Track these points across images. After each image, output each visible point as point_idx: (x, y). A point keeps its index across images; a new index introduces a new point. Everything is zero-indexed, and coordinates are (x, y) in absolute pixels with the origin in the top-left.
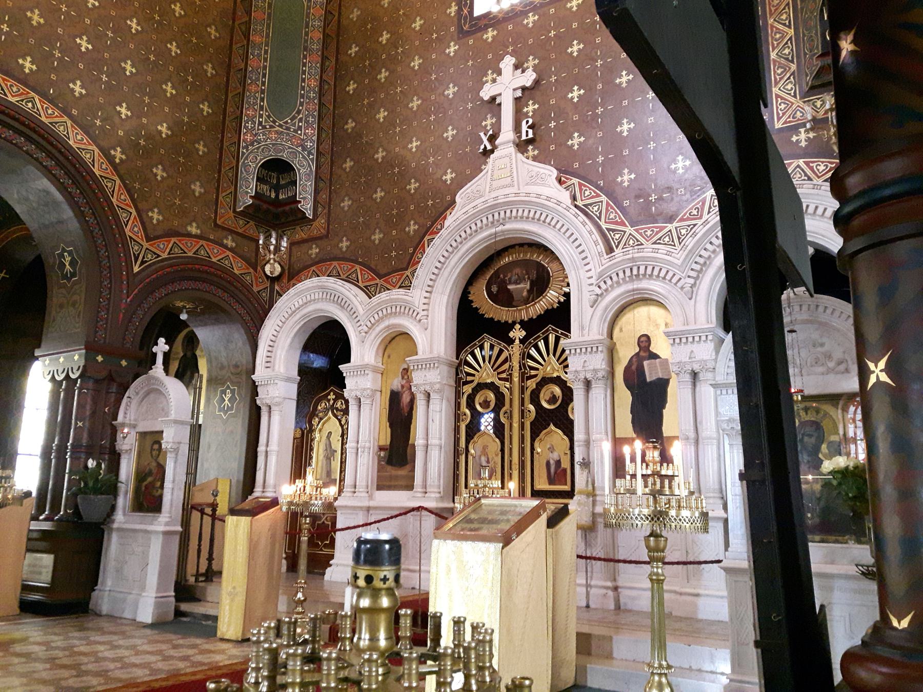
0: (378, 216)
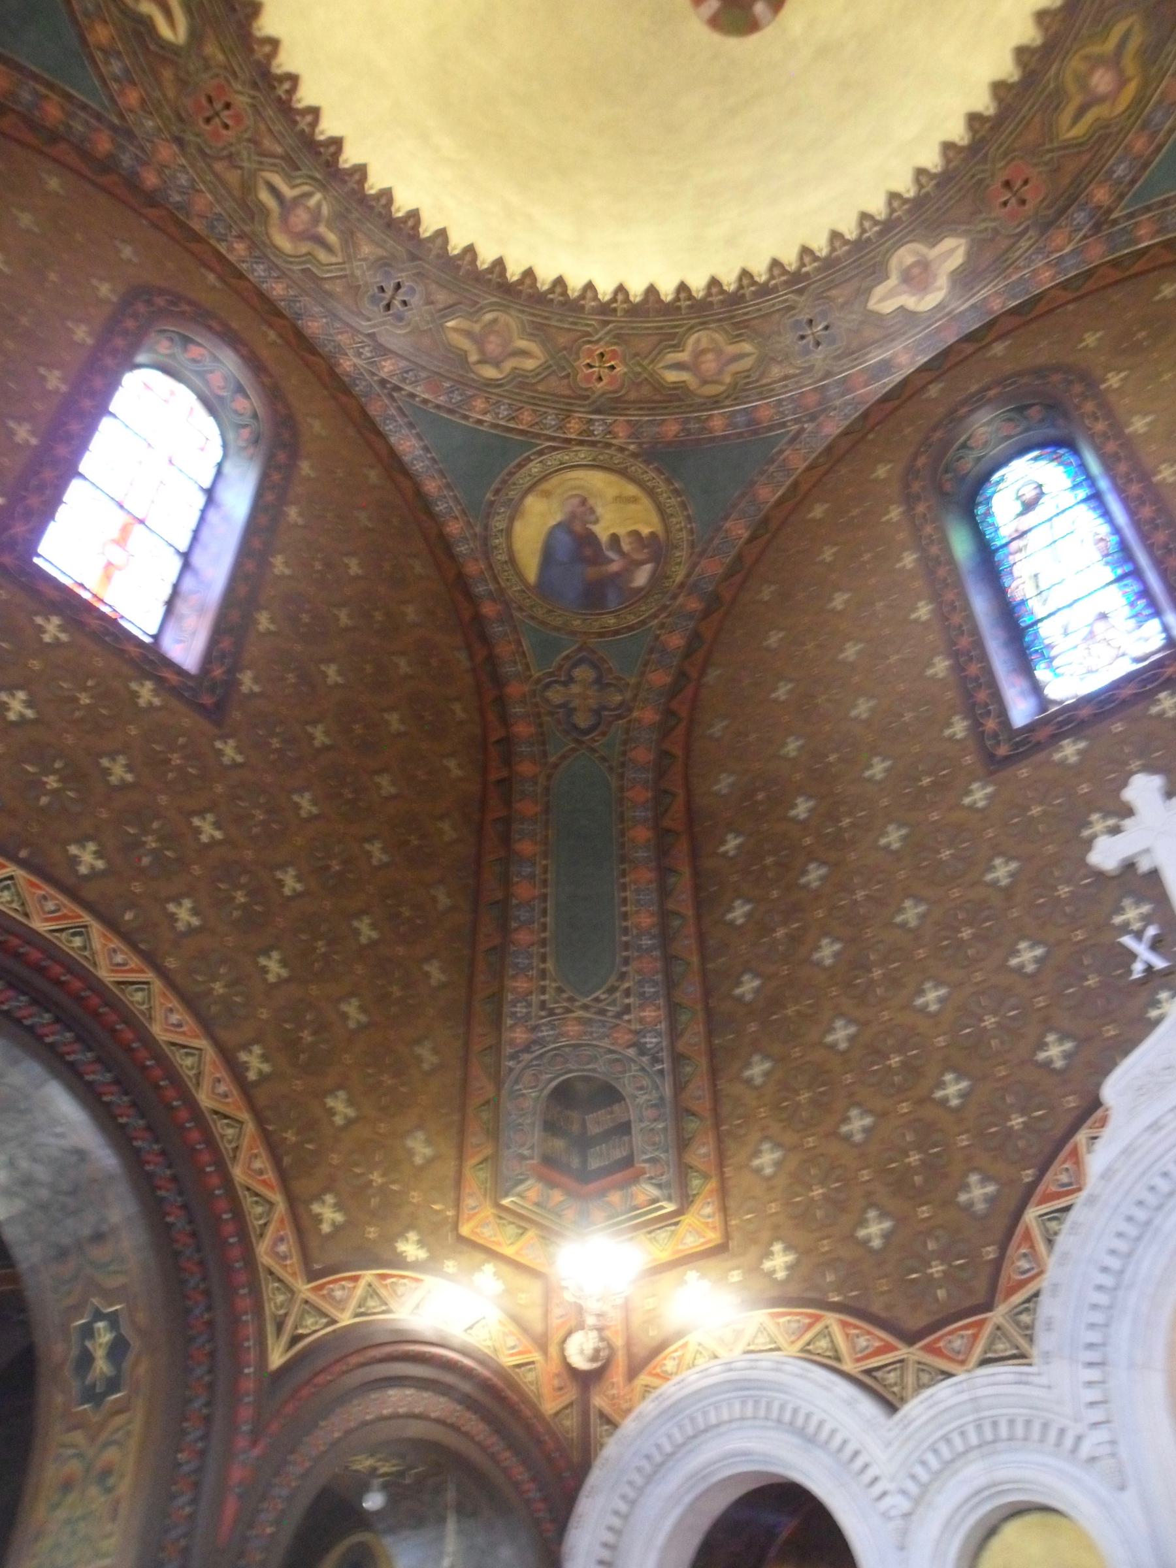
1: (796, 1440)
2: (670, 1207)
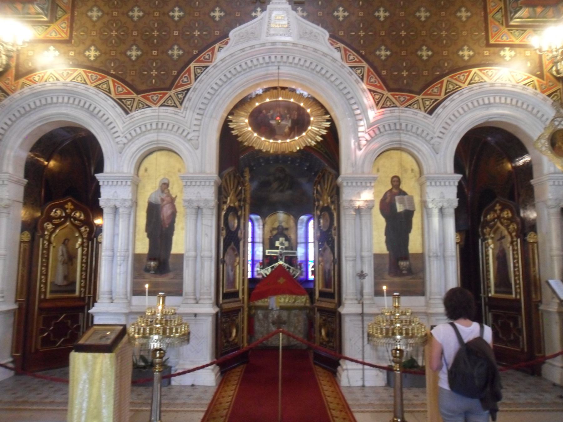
0: (135, 33)
1: (88, 115)
2: (46, 19)
